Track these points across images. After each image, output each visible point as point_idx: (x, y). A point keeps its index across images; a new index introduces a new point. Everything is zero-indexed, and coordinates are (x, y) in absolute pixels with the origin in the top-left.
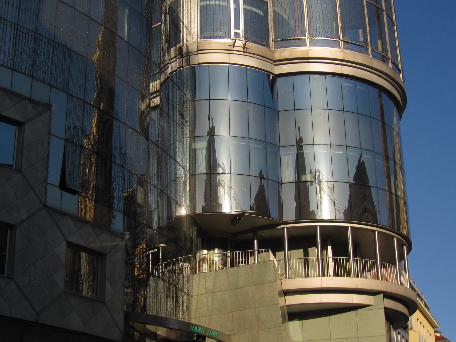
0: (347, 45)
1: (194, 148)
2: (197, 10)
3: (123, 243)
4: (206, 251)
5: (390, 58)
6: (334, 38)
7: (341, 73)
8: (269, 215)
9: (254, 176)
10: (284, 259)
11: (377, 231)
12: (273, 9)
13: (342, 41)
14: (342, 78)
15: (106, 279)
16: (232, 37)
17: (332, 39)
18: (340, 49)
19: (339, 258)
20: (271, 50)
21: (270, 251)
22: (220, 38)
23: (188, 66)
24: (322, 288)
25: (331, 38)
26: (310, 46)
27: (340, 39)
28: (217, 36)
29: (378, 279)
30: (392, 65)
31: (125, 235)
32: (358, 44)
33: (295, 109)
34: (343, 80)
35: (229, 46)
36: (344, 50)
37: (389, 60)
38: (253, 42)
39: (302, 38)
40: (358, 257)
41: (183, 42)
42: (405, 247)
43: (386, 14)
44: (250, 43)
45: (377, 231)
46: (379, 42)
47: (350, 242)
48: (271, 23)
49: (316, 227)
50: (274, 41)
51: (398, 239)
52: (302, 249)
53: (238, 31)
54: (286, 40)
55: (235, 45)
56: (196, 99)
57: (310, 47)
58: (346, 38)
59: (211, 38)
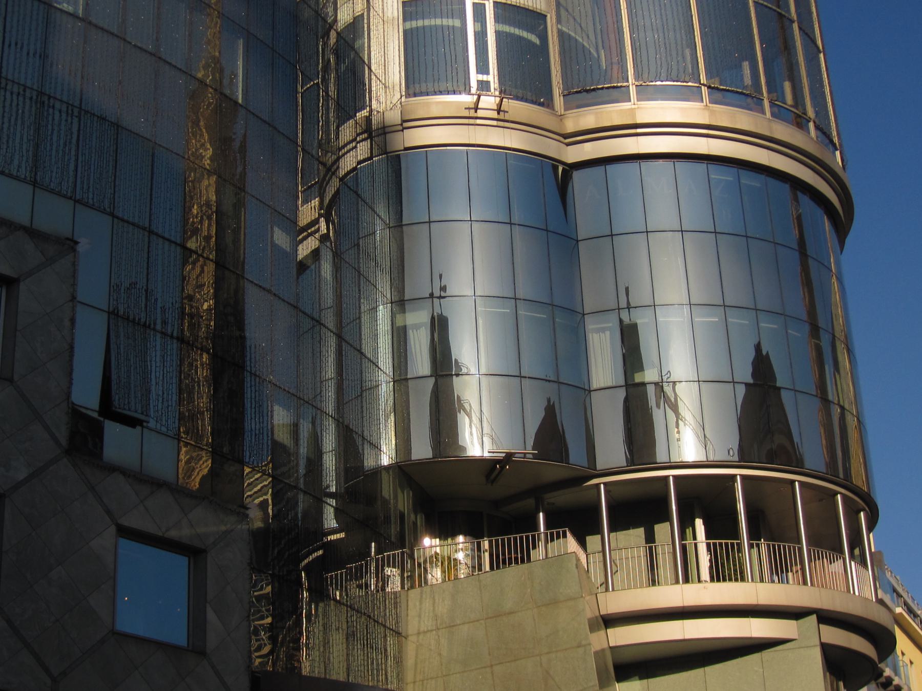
0: (718, 95)
2: (397, 38)
3: (244, 527)
4: (438, 540)
9: (529, 378)
10: (601, 549)
11: (798, 481)
12: (558, 29)
13: (706, 88)
14: (709, 165)
15: (208, 605)
16: (474, 90)
17: (685, 84)
18: (702, 104)
21: (568, 534)
22: (448, 94)
23: (383, 156)
24: (684, 607)
25: (681, 82)
26: (638, 100)
27: (700, 84)
29: (805, 583)
30: (816, 133)
33: (613, 234)
34: (712, 167)
35: (466, 109)
36: (711, 105)
37: (810, 121)
38: (517, 98)
40: (762, 540)
41: (370, 106)
42: (862, 513)
43: (800, 28)
44: (510, 101)
45: (798, 481)
46: (787, 86)
47: (741, 506)
48: (555, 58)
49: (667, 477)
50: (564, 96)
51: (844, 497)
53: (484, 78)
54: (587, 91)
55: (479, 107)
56: (403, 223)
57: (639, 103)
59: (428, 95)
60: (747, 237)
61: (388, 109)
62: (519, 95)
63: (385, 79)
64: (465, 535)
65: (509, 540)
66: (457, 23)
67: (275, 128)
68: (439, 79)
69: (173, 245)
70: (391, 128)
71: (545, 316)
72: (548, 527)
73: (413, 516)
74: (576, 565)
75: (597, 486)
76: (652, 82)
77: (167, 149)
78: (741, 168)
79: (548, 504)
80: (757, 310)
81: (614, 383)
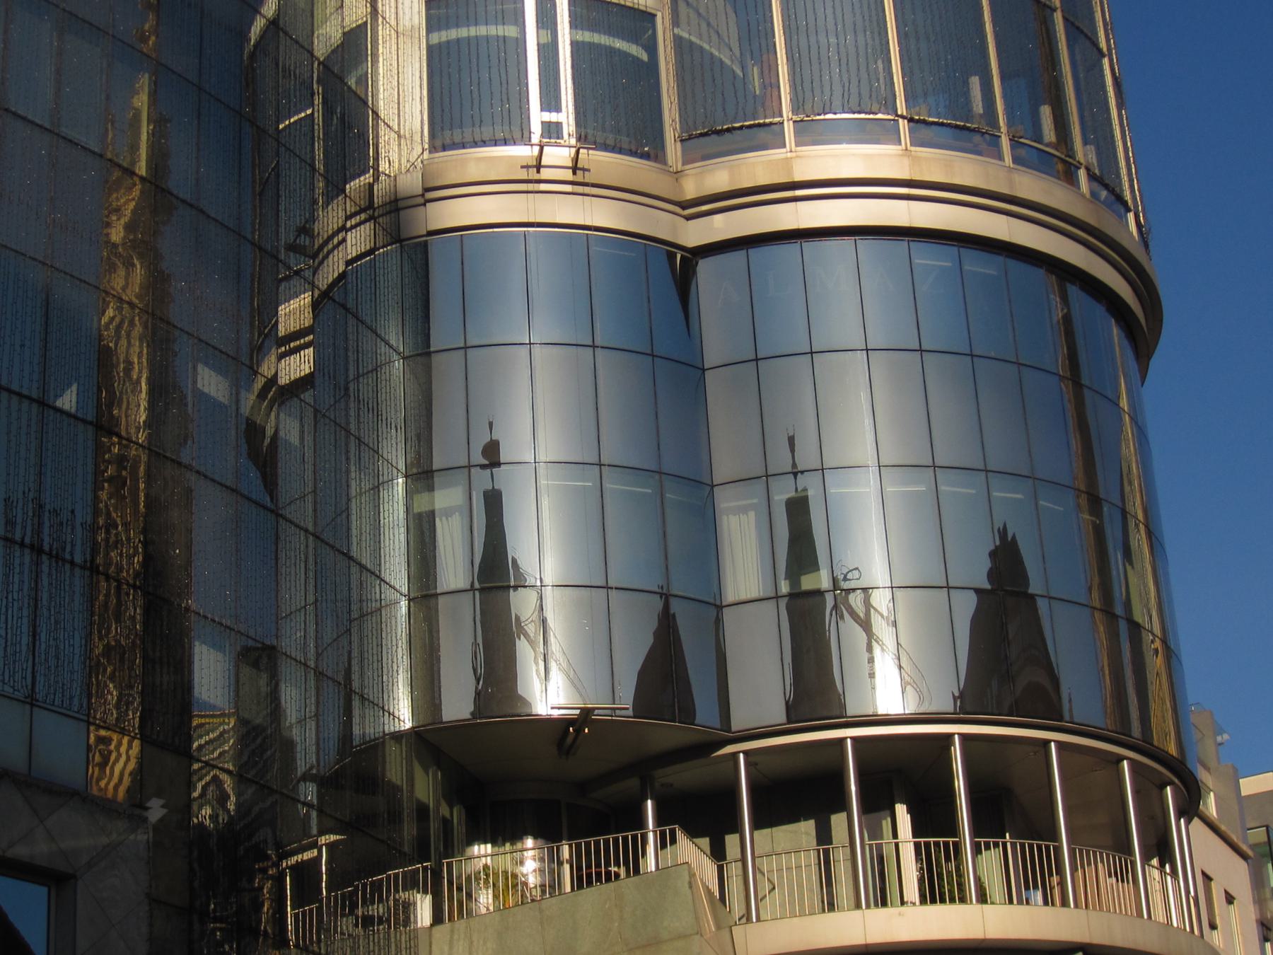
1: (431, 508)
2: (418, 59)
3: (139, 837)
4: (489, 846)
5: (1081, 164)
6: (876, 114)
7: (907, 224)
8: (687, 714)
9: (616, 588)
12: (674, 35)
13: (906, 121)
14: (911, 243)
16: (536, 138)
17: (871, 116)
18: (899, 147)
19: (934, 842)
20: (671, 170)
21: (679, 834)
22: (496, 145)
23: (394, 246)
24: (866, 946)
25: (866, 113)
26: (797, 145)
27: (897, 116)
28: (484, 139)
30: (1090, 186)
31: (147, 809)
32: (962, 124)
33: (759, 357)
34: (918, 247)
35: (522, 167)
36: (913, 149)
37: (1079, 168)
38: (605, 147)
39: (771, 120)
40: (1007, 835)
41: (376, 168)
42: (1168, 788)
43: (1065, 19)
44: (591, 152)
45: (1054, 741)
46: (1046, 112)
47: (960, 784)
48: (668, 81)
49: (842, 741)
50: (681, 141)
51: (1136, 767)
52: (811, 819)
53: (552, 117)
54: (719, 132)
55: (542, 164)
56: (432, 349)
57: (799, 148)
58: (917, 108)
59: (464, 147)
60: (972, 356)
61: (403, 170)
62: (608, 142)
63: (399, 125)
64: (535, 837)
65: (607, 842)
66: (511, 31)
67: (202, 211)
68: (481, 121)
69: (26, 404)
70: (409, 200)
71: (650, 491)
72: (660, 821)
73: (445, 810)
74: (690, 883)
75: (734, 756)
76: (819, 115)
77: (16, 252)
78: (963, 247)
79: (662, 785)
80: (987, 471)
81: (761, 594)
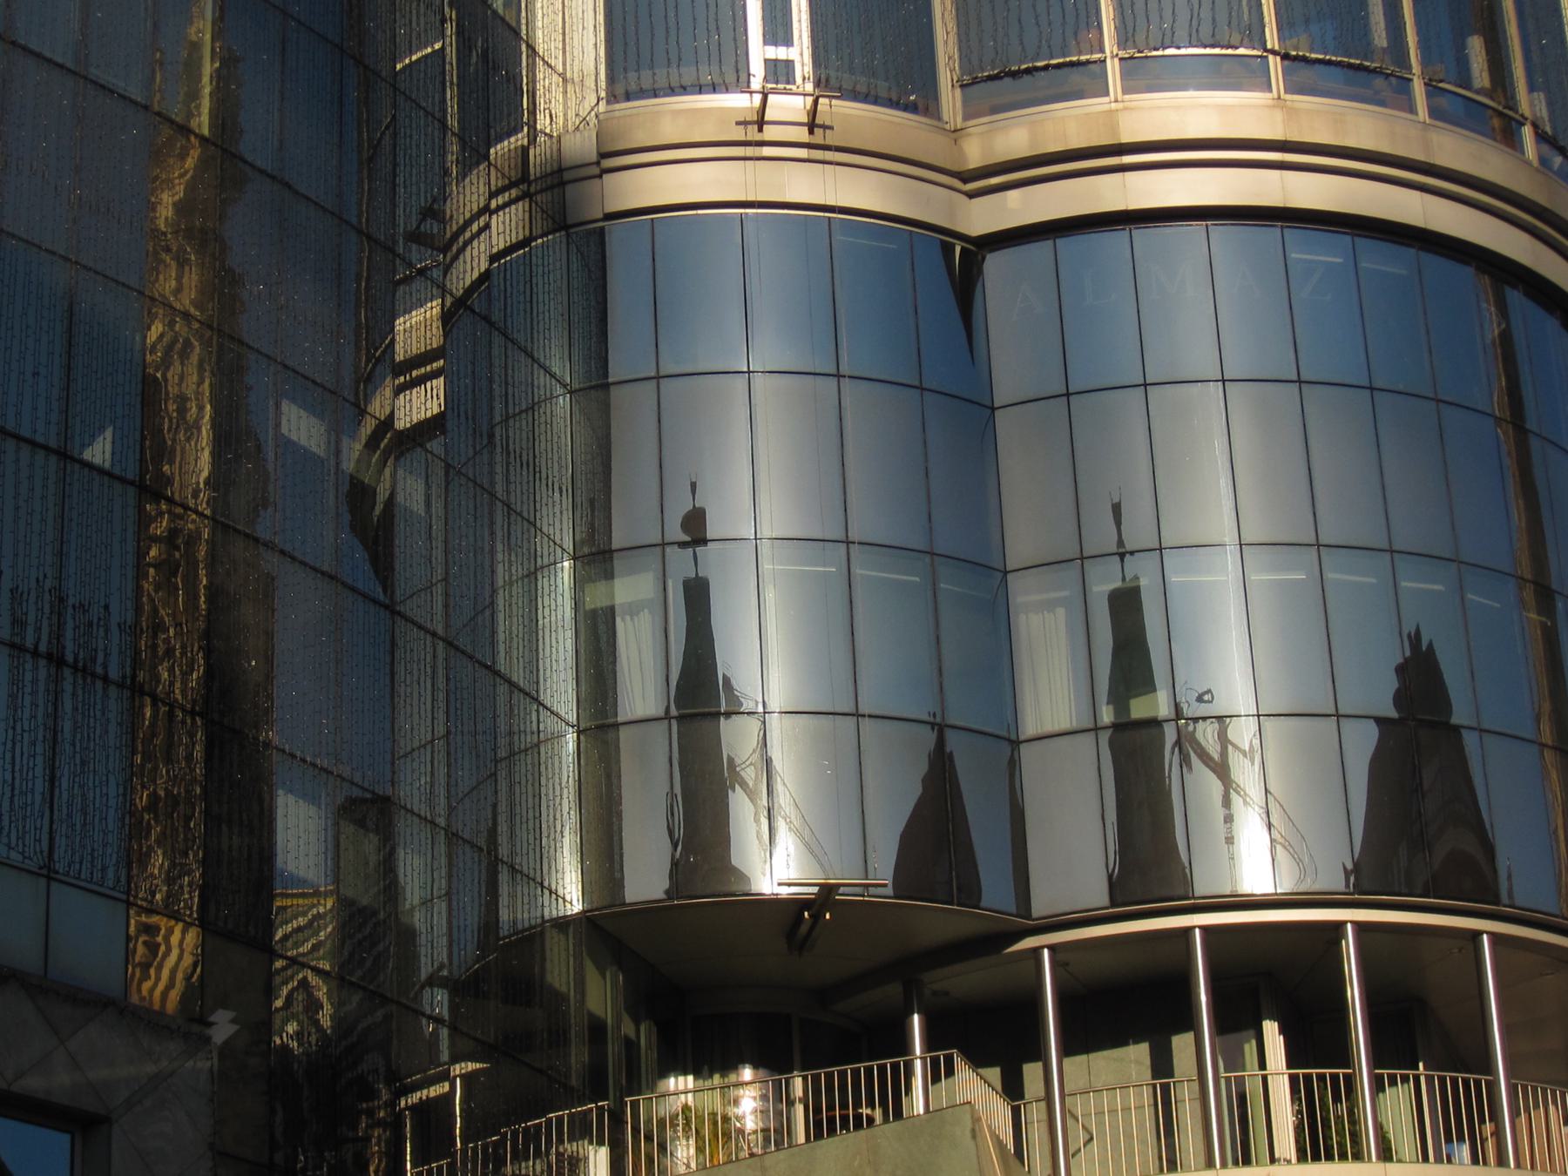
0: (1306, 74)
1: (609, 603)
3: (199, 1065)
4: (690, 1078)
5: (1526, 119)
6: (1237, 48)
7: (1282, 205)
8: (969, 892)
9: (870, 716)
10: (1043, 1094)
13: (1278, 58)
14: (1285, 230)
16: (756, 83)
17: (1230, 51)
18: (1268, 95)
20: (947, 127)
22: (700, 92)
25: (1222, 47)
26: (1125, 92)
27: (1266, 50)
28: (684, 84)
30: (1538, 149)
31: (210, 1024)
32: (1358, 62)
33: (1070, 391)
34: (1293, 235)
35: (738, 123)
36: (1289, 97)
37: (1524, 124)
38: (855, 96)
39: (1088, 57)
40: (1421, 1065)
41: (532, 125)
44: (834, 102)
45: (1487, 933)
46: (1476, 46)
47: (1354, 993)
49: (1188, 931)
50: (961, 86)
53: (781, 53)
54: (1014, 75)
55: (766, 118)
57: (1127, 97)
58: (1295, 40)
59: (656, 96)
60: (1372, 389)
61: (571, 128)
62: (858, 88)
63: (564, 64)
64: (756, 1066)
65: (856, 1073)
67: (288, 186)
68: (680, 59)
69: (41, 454)
71: (917, 579)
72: (931, 1043)
73: (628, 1028)
74: (973, 1131)
75: (1036, 952)
76: (1158, 50)
77: (27, 242)
78: (1359, 236)
79: (935, 993)
80: (1392, 552)
81: (1074, 724)
